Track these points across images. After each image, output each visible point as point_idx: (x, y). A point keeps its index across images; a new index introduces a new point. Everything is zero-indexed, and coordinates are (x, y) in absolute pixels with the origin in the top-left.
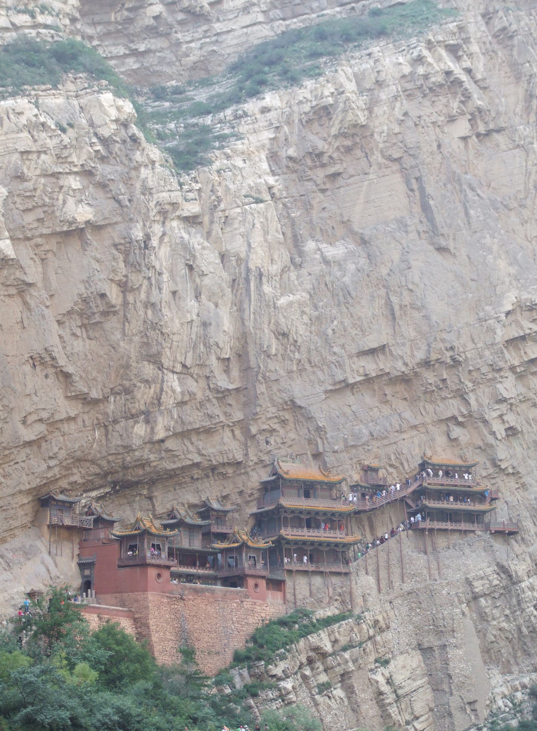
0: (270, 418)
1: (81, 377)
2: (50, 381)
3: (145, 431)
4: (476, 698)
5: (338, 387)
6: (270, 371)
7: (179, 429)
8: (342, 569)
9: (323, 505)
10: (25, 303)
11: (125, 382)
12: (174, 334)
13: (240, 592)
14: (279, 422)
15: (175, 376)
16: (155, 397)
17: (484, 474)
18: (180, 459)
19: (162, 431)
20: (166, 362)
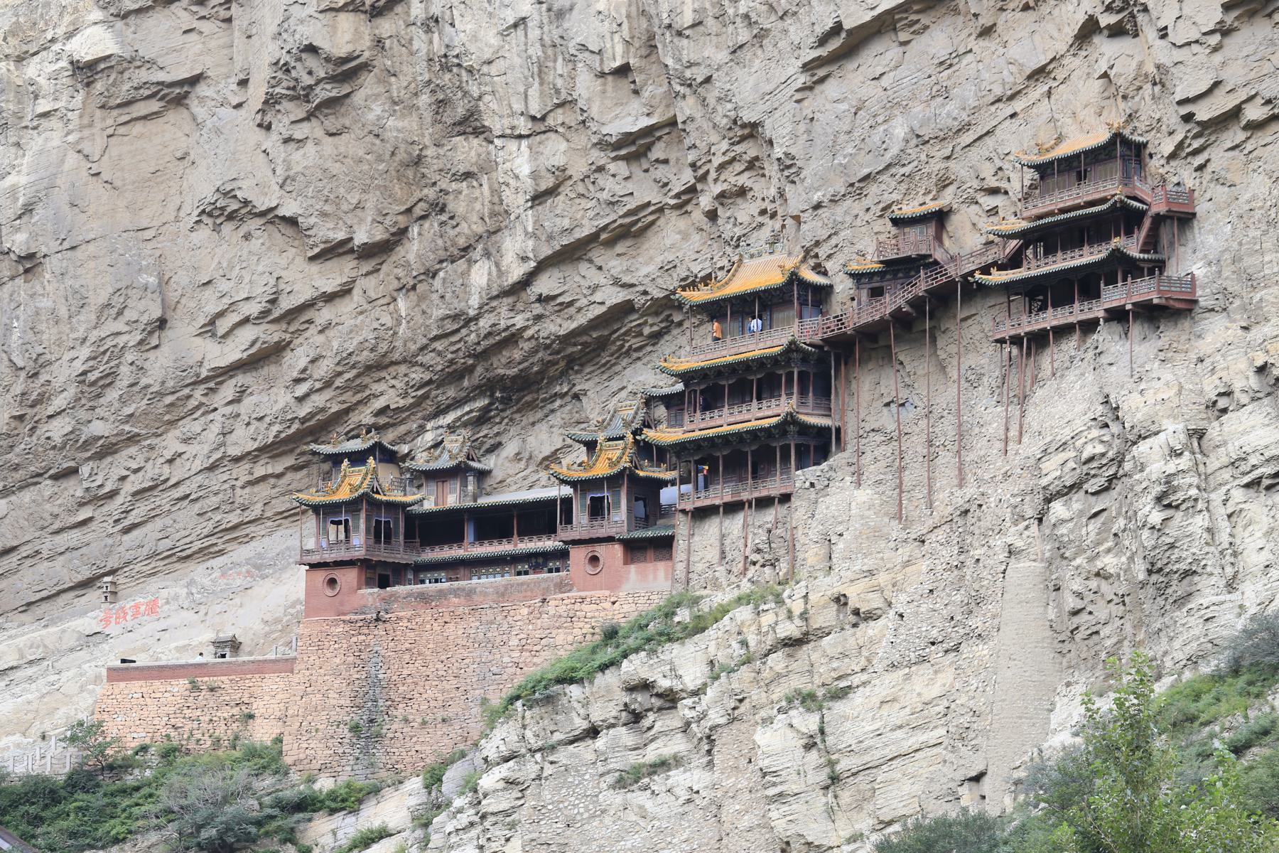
0: (722, 167)
1: (324, 215)
2: (255, 244)
3: (489, 274)
4: (981, 768)
5: (834, 44)
6: (691, 65)
7: (546, 251)
8: (773, 487)
9: (761, 345)
10: (194, 119)
11: (426, 191)
12: (490, 63)
13: (538, 583)
14: (747, 169)
15: (524, 143)
16: (496, 200)
17: (1168, 148)
18: (579, 310)
19: (514, 265)
20: (497, 125)
